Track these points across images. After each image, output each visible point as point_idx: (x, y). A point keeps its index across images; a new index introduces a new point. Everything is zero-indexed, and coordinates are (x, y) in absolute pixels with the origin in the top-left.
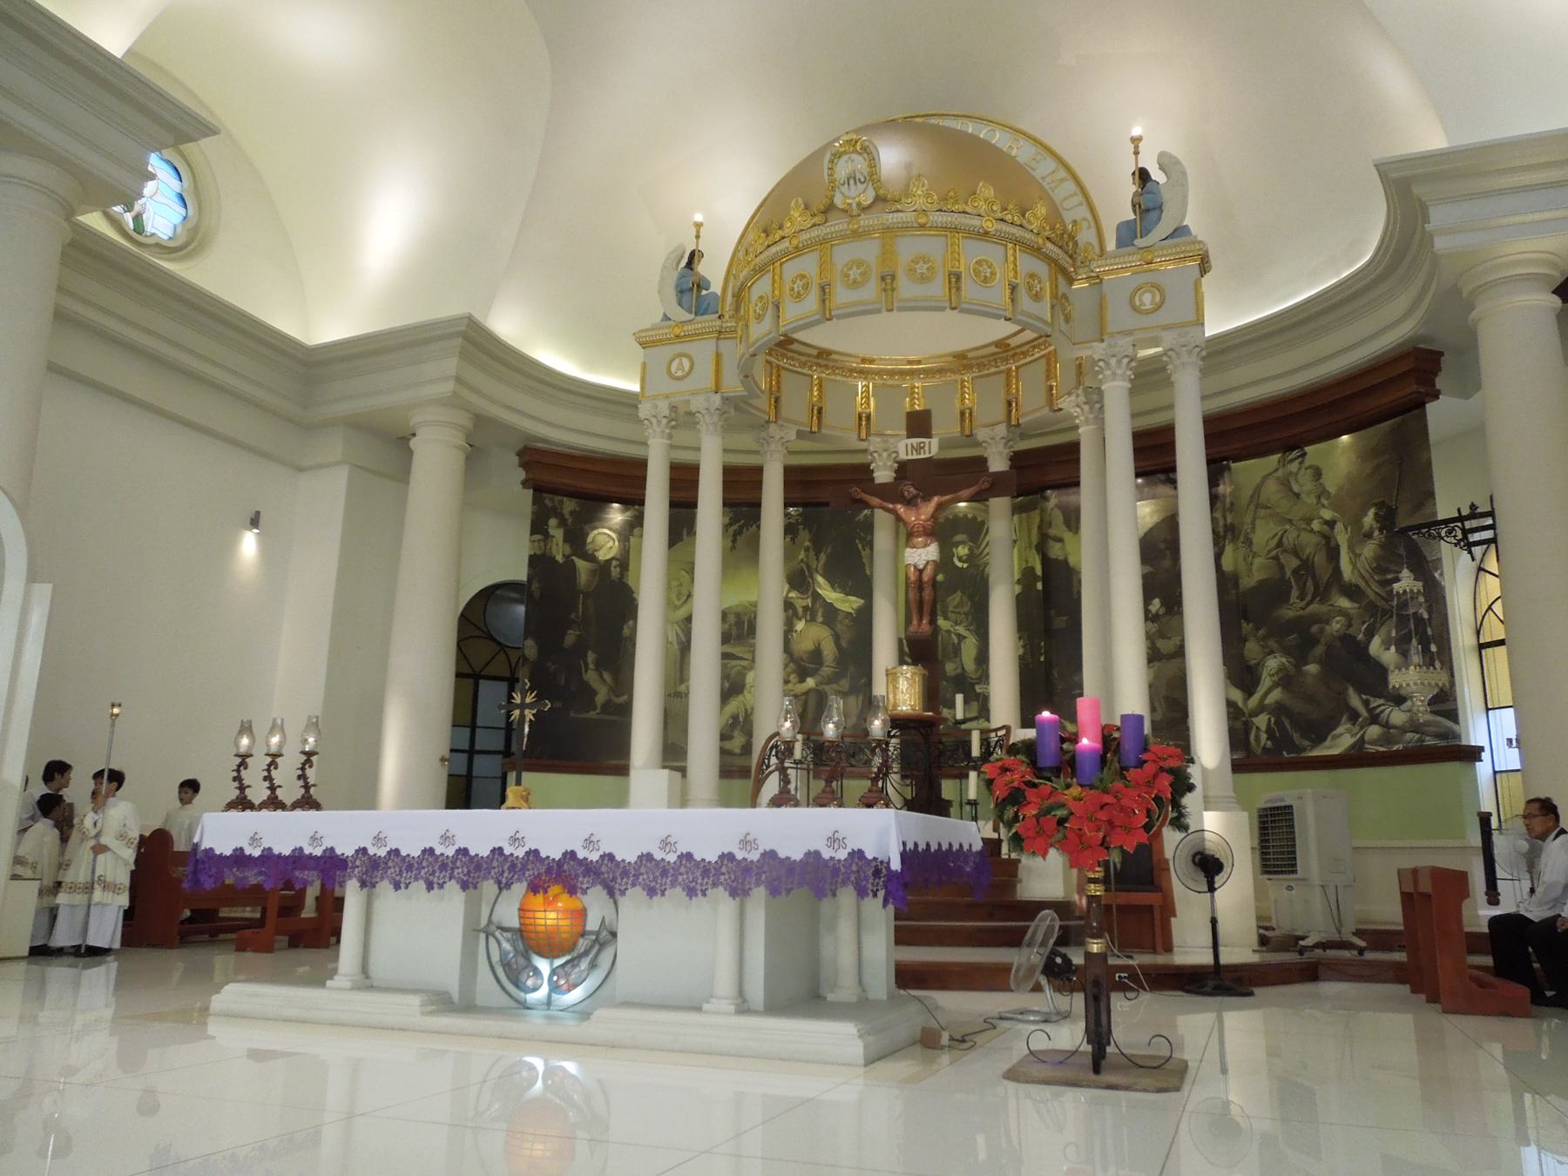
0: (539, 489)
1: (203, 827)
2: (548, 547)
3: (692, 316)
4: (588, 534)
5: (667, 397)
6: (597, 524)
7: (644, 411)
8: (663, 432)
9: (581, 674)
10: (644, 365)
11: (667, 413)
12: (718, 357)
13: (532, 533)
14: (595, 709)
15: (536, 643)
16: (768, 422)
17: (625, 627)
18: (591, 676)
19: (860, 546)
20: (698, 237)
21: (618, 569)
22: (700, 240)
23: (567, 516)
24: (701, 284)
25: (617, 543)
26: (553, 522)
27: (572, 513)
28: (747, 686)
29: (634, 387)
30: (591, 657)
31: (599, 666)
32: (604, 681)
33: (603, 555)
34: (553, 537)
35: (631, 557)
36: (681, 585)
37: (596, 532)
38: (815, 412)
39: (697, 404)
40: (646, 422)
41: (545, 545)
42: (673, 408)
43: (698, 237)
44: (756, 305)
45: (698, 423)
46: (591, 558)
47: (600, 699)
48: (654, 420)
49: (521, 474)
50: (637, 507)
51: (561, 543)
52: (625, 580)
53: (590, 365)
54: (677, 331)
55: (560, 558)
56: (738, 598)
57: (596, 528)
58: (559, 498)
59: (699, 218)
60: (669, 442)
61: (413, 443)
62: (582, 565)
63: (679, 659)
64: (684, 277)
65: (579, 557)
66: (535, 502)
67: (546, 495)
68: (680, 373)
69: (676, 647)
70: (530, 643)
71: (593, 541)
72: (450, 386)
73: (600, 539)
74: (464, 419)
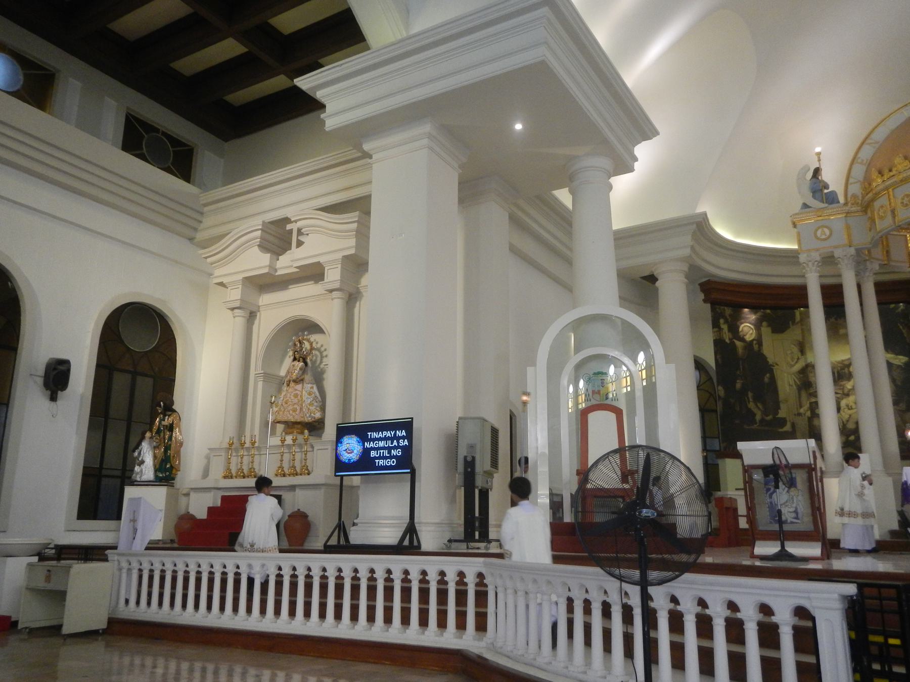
0: (714, 304)
1: (906, 474)
2: (721, 334)
3: (826, 205)
4: (738, 327)
5: (817, 250)
6: (743, 321)
7: (803, 258)
8: (816, 269)
9: (747, 404)
10: (799, 234)
11: (818, 258)
12: (848, 228)
13: (713, 328)
14: (756, 423)
15: (724, 388)
16: (867, 260)
17: (765, 377)
18: (751, 405)
19: (901, 327)
20: (819, 160)
21: (757, 346)
22: (821, 162)
23: (728, 317)
24: (826, 186)
25: (754, 331)
26: (722, 321)
27: (730, 315)
28: (842, 408)
29: (796, 247)
30: (750, 395)
31: (757, 399)
32: (759, 408)
33: (749, 338)
34: (723, 329)
35: (763, 337)
36: (792, 353)
37: (743, 325)
38: (885, 253)
39: (838, 253)
40: (804, 265)
41: (720, 334)
42: (820, 255)
43: (819, 160)
44: (903, 199)
45: (837, 264)
46: (742, 339)
47: (758, 417)
48: (810, 264)
49: (702, 296)
50: (762, 310)
51: (727, 332)
52: (762, 352)
53: (738, 233)
54: (820, 214)
55: (727, 341)
56: (842, 356)
57: (742, 323)
58: (722, 307)
59: (818, 150)
60: (818, 275)
61: (657, 284)
62: (739, 344)
63: (797, 394)
64: (815, 183)
65: (736, 339)
66: (713, 310)
67: (718, 307)
68: (824, 237)
69: (795, 387)
70: (720, 388)
71: (742, 330)
72: (687, 252)
73: (746, 329)
74: (685, 268)
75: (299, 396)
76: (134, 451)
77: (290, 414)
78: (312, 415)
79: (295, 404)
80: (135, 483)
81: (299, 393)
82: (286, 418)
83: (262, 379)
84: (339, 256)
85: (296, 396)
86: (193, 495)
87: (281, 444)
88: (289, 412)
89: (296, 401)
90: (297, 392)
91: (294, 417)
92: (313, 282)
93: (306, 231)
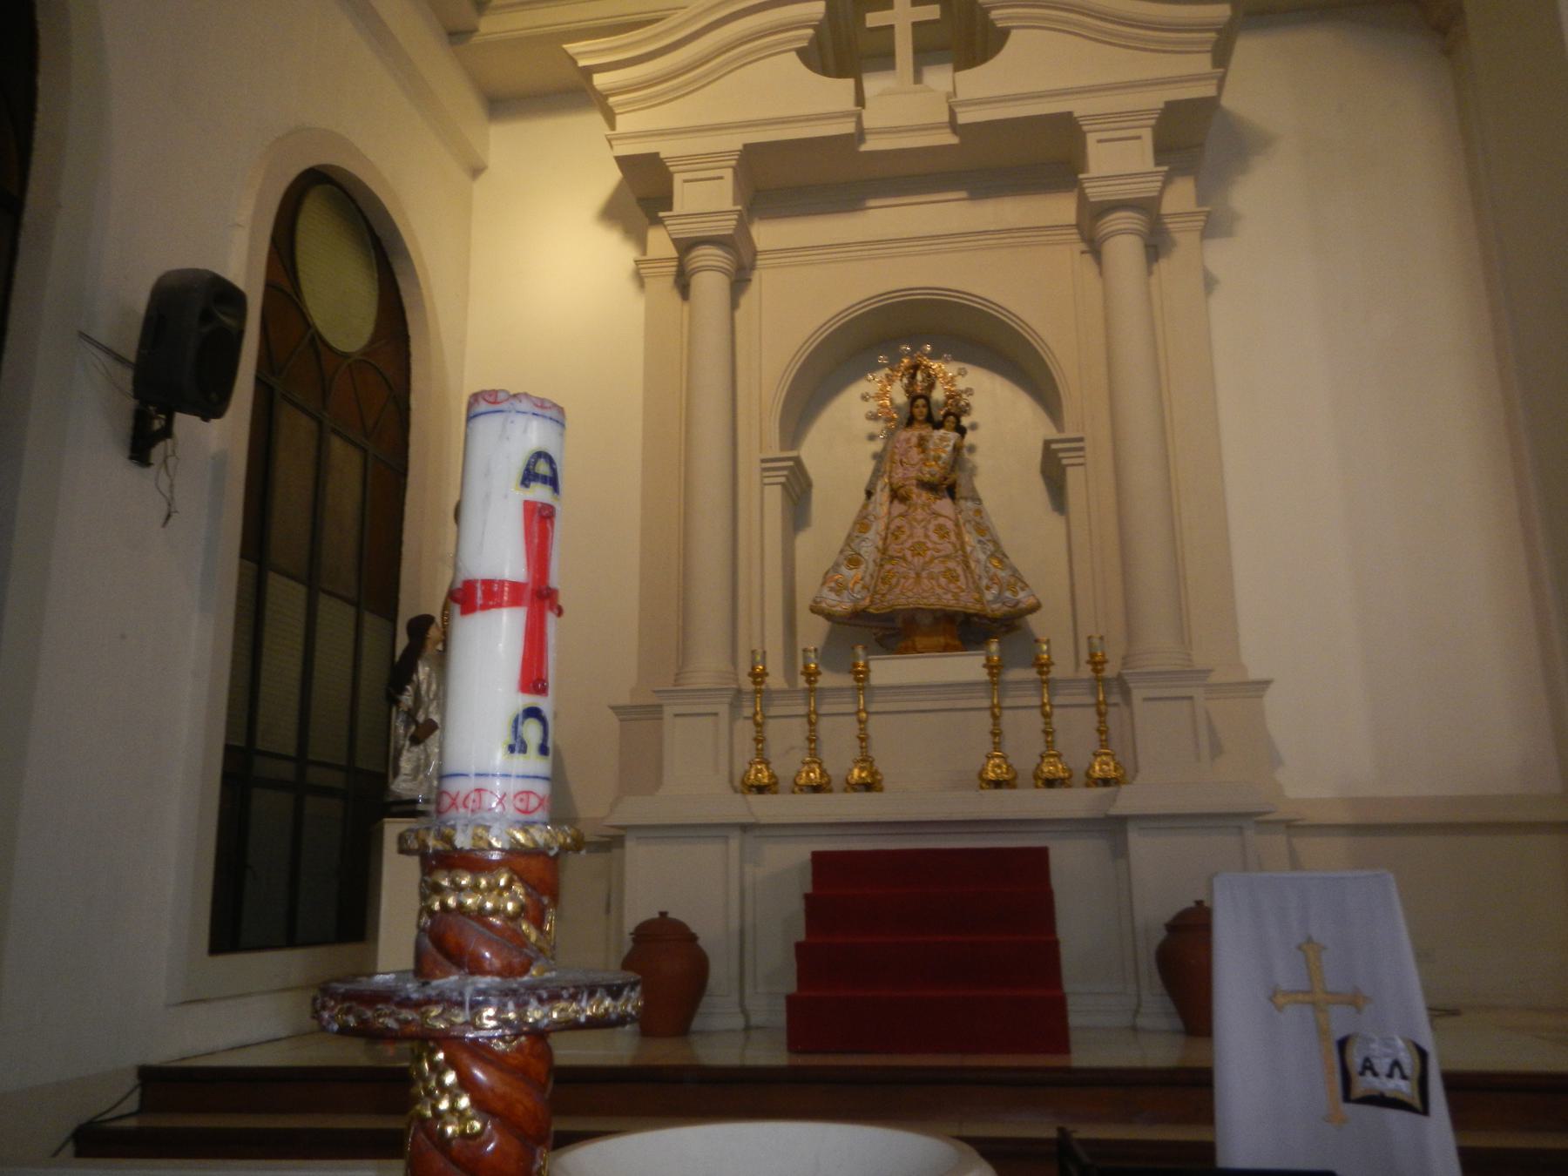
75: (953, 538)
76: (402, 690)
77: (939, 586)
78: (1008, 594)
79: (947, 557)
80: (395, 809)
81: (950, 525)
82: (933, 600)
83: (783, 480)
84: (1156, 99)
85: (942, 532)
86: (635, 852)
87: (987, 678)
88: (937, 581)
89: (947, 548)
90: (941, 520)
91: (940, 599)
92: (963, 194)
93: (1009, 18)
